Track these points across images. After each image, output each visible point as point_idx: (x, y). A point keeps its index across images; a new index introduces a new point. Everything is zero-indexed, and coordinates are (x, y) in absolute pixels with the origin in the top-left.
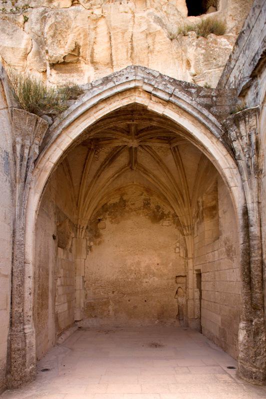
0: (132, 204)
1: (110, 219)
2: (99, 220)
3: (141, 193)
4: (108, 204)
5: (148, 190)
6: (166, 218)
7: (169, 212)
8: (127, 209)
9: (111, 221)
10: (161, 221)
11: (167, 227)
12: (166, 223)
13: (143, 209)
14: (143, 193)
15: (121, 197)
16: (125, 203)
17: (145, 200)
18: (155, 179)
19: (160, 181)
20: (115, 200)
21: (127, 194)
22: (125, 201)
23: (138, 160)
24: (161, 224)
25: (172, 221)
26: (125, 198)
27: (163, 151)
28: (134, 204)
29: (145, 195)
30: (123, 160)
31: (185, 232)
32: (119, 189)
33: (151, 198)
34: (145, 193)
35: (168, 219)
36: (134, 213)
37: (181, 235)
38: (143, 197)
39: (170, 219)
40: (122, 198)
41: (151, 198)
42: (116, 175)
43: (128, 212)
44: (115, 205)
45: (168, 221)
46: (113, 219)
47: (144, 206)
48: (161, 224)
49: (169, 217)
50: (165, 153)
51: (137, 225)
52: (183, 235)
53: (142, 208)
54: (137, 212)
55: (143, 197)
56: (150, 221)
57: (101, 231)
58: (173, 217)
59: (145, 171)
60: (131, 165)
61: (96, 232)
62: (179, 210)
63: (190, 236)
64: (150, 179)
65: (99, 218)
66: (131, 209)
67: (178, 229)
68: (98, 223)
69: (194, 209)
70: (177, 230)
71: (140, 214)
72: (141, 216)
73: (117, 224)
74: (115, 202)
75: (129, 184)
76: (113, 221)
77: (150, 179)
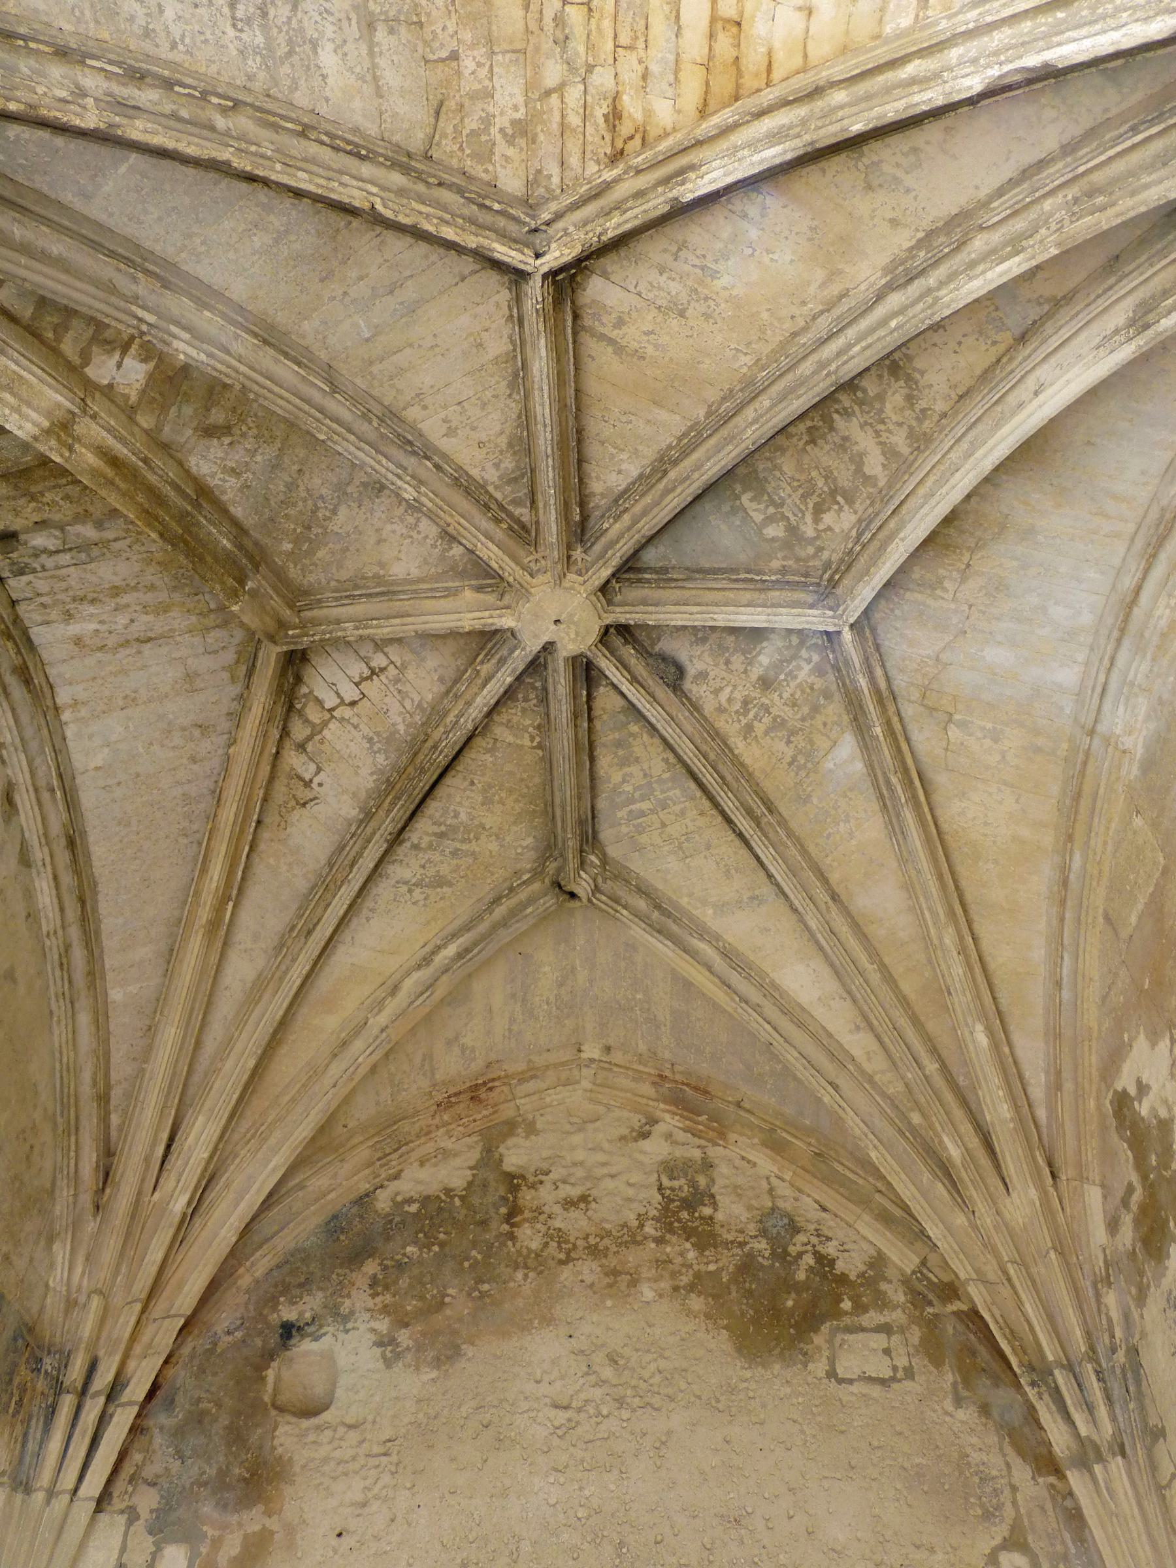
0: (569, 1204)
1: (383, 1325)
2: (288, 1331)
3: (636, 1120)
4: (383, 1202)
5: (690, 1098)
6: (860, 1308)
7: (878, 1262)
8: (529, 1237)
9: (385, 1342)
10: (818, 1339)
11: (876, 1391)
12: (862, 1353)
13: (660, 1241)
14: (652, 1121)
15: (488, 1150)
16: (514, 1189)
17: (670, 1168)
18: (735, 979)
19: (772, 991)
20: (440, 1169)
21: (531, 1129)
22: (513, 1182)
23: (606, 834)
24: (819, 1367)
25: (915, 1335)
26: (516, 1155)
27: (778, 724)
28: (584, 1198)
29: (669, 1136)
30: (490, 823)
31: (1059, 1438)
32: (477, 1092)
33: (715, 1152)
34: (670, 1122)
35: (872, 1318)
36: (589, 1269)
37: (1022, 1473)
38: (655, 1149)
39: (896, 1317)
40: (489, 1158)
41: (715, 1152)
42: (451, 950)
43: (535, 1262)
44: (433, 1215)
45: (879, 1341)
46: (403, 1323)
47: (666, 1209)
48: (819, 1367)
49: (882, 1303)
50: (799, 741)
51: (608, 1373)
52: (1047, 1464)
53: (649, 1229)
54: (613, 1261)
55: (655, 1149)
56: (721, 1341)
57: (287, 1436)
58: (918, 1299)
59: (664, 916)
60: (552, 867)
61: (236, 1437)
62: (960, 1220)
63: (1117, 1464)
64: (699, 977)
65: (289, 1314)
66: (560, 1237)
67: (985, 1409)
68: (269, 1356)
69: (1094, 1196)
70: (967, 1415)
71: (634, 1283)
72: (648, 1293)
73: (437, 1362)
74: (433, 1189)
75: (553, 1057)
76: (404, 1337)
77: (699, 977)
